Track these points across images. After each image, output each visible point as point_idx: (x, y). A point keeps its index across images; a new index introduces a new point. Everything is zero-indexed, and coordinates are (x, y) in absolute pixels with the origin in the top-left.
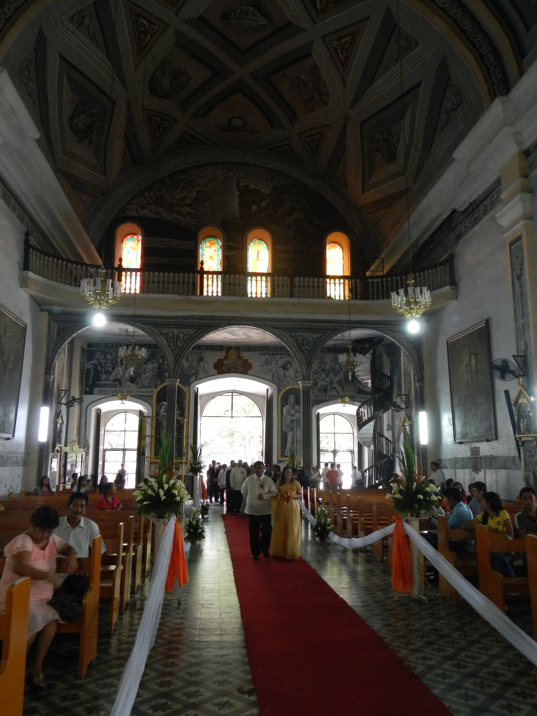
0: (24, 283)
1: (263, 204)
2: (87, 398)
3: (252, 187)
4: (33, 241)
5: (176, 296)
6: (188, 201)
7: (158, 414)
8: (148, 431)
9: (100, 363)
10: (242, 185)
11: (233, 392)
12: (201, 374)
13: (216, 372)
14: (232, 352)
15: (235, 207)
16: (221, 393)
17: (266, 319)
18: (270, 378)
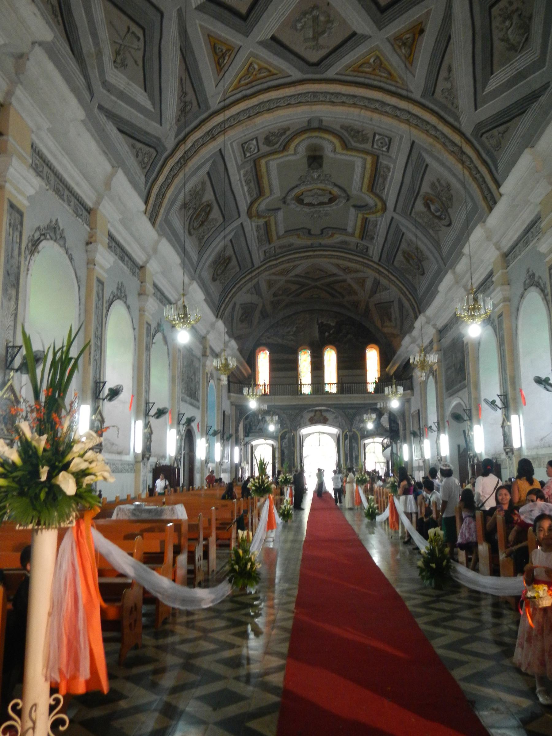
0: (229, 398)
1: (331, 332)
2: (247, 439)
3: (325, 322)
4: (231, 380)
5: (290, 396)
6: (292, 333)
7: (281, 447)
8: (277, 455)
9: (251, 421)
10: (320, 322)
11: (319, 433)
12: (302, 425)
13: (309, 423)
14: (317, 413)
15: (316, 334)
16: (313, 433)
17: (332, 404)
18: (338, 424)
